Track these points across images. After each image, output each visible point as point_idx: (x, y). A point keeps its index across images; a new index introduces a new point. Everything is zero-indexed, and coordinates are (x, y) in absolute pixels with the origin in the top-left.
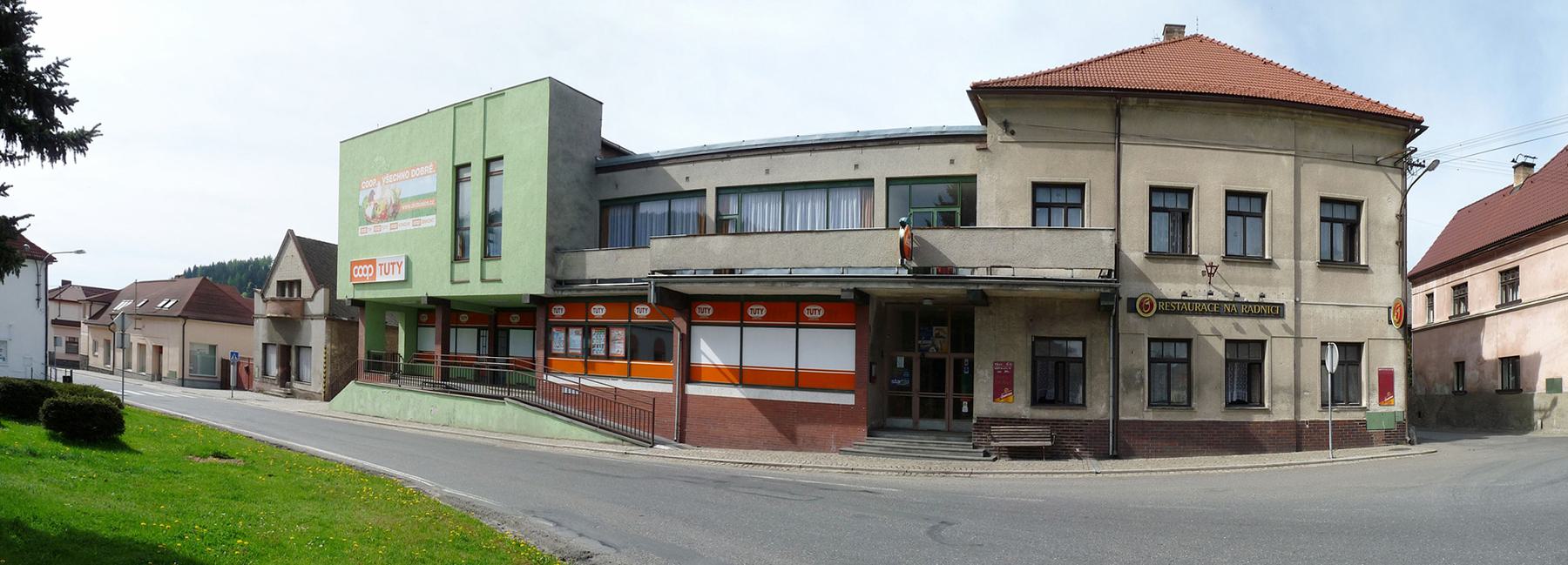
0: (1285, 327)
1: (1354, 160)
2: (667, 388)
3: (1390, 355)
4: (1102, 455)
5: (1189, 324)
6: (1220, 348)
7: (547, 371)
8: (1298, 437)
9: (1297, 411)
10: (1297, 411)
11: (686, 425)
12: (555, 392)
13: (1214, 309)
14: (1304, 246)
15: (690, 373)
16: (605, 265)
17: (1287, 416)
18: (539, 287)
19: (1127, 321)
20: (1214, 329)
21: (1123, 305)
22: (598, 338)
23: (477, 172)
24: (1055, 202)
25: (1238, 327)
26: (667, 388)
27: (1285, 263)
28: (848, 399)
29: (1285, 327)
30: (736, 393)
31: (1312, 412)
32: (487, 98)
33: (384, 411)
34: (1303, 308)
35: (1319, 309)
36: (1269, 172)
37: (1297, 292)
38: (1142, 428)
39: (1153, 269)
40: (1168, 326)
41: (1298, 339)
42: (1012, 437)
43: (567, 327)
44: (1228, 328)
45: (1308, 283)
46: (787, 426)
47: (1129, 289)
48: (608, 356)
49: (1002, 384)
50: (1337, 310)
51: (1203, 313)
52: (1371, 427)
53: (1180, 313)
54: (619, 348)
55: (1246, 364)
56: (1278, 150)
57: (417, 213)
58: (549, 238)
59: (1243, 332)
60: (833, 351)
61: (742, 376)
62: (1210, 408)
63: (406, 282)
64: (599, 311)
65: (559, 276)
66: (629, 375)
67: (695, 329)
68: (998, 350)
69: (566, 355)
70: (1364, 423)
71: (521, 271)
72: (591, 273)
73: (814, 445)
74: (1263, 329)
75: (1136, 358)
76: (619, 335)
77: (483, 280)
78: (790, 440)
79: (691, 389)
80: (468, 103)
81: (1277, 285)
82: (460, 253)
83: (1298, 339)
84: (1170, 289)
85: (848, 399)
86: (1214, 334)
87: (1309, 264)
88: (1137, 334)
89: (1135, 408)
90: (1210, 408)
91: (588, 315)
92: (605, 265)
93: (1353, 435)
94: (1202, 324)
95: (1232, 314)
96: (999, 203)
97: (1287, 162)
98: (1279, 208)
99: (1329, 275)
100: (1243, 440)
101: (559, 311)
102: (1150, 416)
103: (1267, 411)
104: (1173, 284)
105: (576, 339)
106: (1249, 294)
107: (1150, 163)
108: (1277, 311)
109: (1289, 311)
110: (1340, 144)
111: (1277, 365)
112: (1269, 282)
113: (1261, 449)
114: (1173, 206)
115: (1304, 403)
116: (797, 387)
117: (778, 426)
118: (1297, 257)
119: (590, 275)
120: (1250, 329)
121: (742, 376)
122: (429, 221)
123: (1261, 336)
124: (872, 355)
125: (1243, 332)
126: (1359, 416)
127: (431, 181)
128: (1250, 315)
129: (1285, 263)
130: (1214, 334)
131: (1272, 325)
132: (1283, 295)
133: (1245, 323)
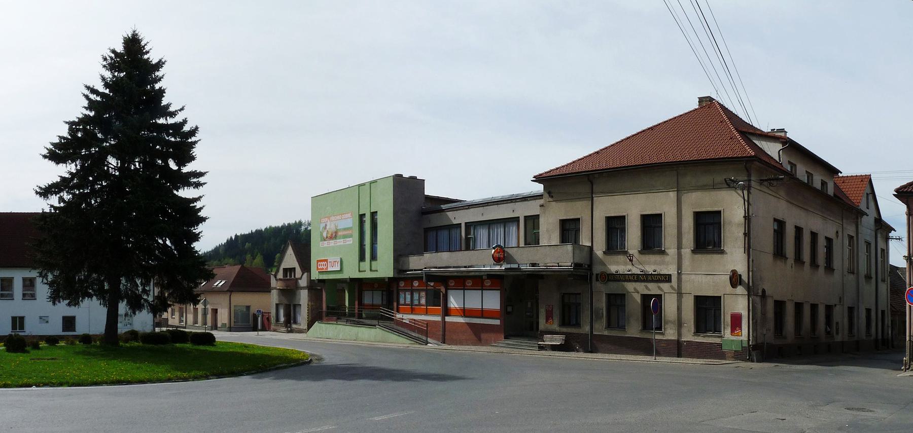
0: (672, 287)
1: (714, 187)
2: (439, 319)
3: (737, 303)
4: (586, 351)
5: (623, 286)
6: (638, 299)
7: (398, 311)
8: (679, 349)
9: (680, 334)
10: (680, 334)
11: (445, 334)
12: (400, 323)
13: (636, 278)
14: (684, 241)
15: (447, 312)
16: (418, 263)
17: (674, 338)
18: (390, 274)
19: (598, 286)
20: (635, 289)
21: (594, 277)
22: (416, 296)
23: (367, 219)
24: (569, 230)
25: (647, 287)
26: (439, 319)
27: (672, 251)
28: (497, 322)
29: (672, 287)
30: (461, 320)
31: (689, 336)
32: (371, 183)
33: (330, 336)
34: (683, 277)
35: (693, 277)
36: (662, 202)
37: (679, 267)
38: (601, 338)
39: (608, 259)
40: (614, 287)
41: (680, 294)
42: (551, 340)
43: (419, 291)
44: (643, 288)
45: (686, 263)
46: (478, 334)
47: (597, 269)
48: (420, 305)
49: (549, 317)
50: (704, 277)
51: (630, 281)
52: (725, 348)
53: (619, 281)
54: (423, 301)
55: (652, 309)
56: (667, 189)
57: (345, 237)
58: (395, 251)
59: (649, 290)
60: (492, 301)
61: (465, 312)
62: (634, 330)
63: (341, 271)
64: (416, 284)
65: (400, 267)
66: (427, 313)
67: (450, 292)
68: (549, 300)
69: (405, 304)
70: (720, 345)
71: (384, 268)
72: (412, 266)
73: (487, 343)
74: (660, 288)
75: (601, 303)
76: (423, 294)
77: (371, 270)
78: (479, 341)
79: (448, 319)
80: (364, 185)
81: (668, 264)
82: (362, 258)
83: (680, 294)
84: (613, 269)
85: (497, 322)
86: (636, 291)
87: (687, 252)
88: (601, 291)
89: (601, 329)
90: (634, 330)
91: (412, 286)
92: (418, 263)
93: (714, 352)
94: (630, 286)
95: (644, 281)
96: (548, 231)
97: (673, 195)
98: (669, 221)
99: (698, 257)
100: (645, 347)
101: (402, 284)
102: (606, 333)
103: (663, 334)
104: (617, 266)
105: (408, 297)
106: (650, 269)
107: (608, 205)
108: (667, 278)
109: (674, 279)
110: (707, 179)
111: (670, 306)
112: (663, 263)
113: (658, 354)
114: (615, 225)
115: (684, 331)
116: (482, 317)
117: (476, 335)
118: (679, 247)
119: (411, 267)
120: (653, 288)
121: (465, 312)
122: (350, 241)
123: (659, 292)
124: (506, 301)
125: (649, 290)
126: (718, 340)
127: (349, 222)
128: (652, 281)
129: (672, 251)
130: (636, 291)
131: (665, 286)
132: (672, 270)
133: (651, 285)
